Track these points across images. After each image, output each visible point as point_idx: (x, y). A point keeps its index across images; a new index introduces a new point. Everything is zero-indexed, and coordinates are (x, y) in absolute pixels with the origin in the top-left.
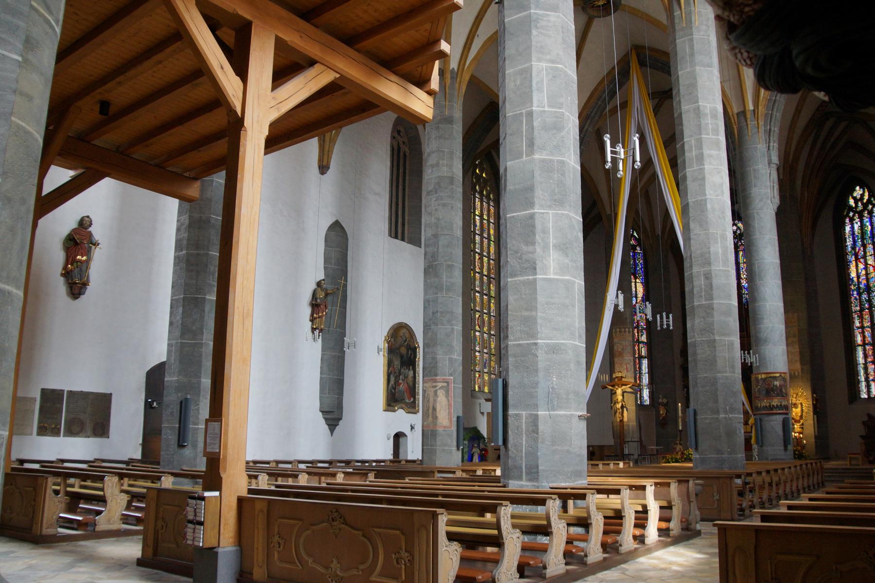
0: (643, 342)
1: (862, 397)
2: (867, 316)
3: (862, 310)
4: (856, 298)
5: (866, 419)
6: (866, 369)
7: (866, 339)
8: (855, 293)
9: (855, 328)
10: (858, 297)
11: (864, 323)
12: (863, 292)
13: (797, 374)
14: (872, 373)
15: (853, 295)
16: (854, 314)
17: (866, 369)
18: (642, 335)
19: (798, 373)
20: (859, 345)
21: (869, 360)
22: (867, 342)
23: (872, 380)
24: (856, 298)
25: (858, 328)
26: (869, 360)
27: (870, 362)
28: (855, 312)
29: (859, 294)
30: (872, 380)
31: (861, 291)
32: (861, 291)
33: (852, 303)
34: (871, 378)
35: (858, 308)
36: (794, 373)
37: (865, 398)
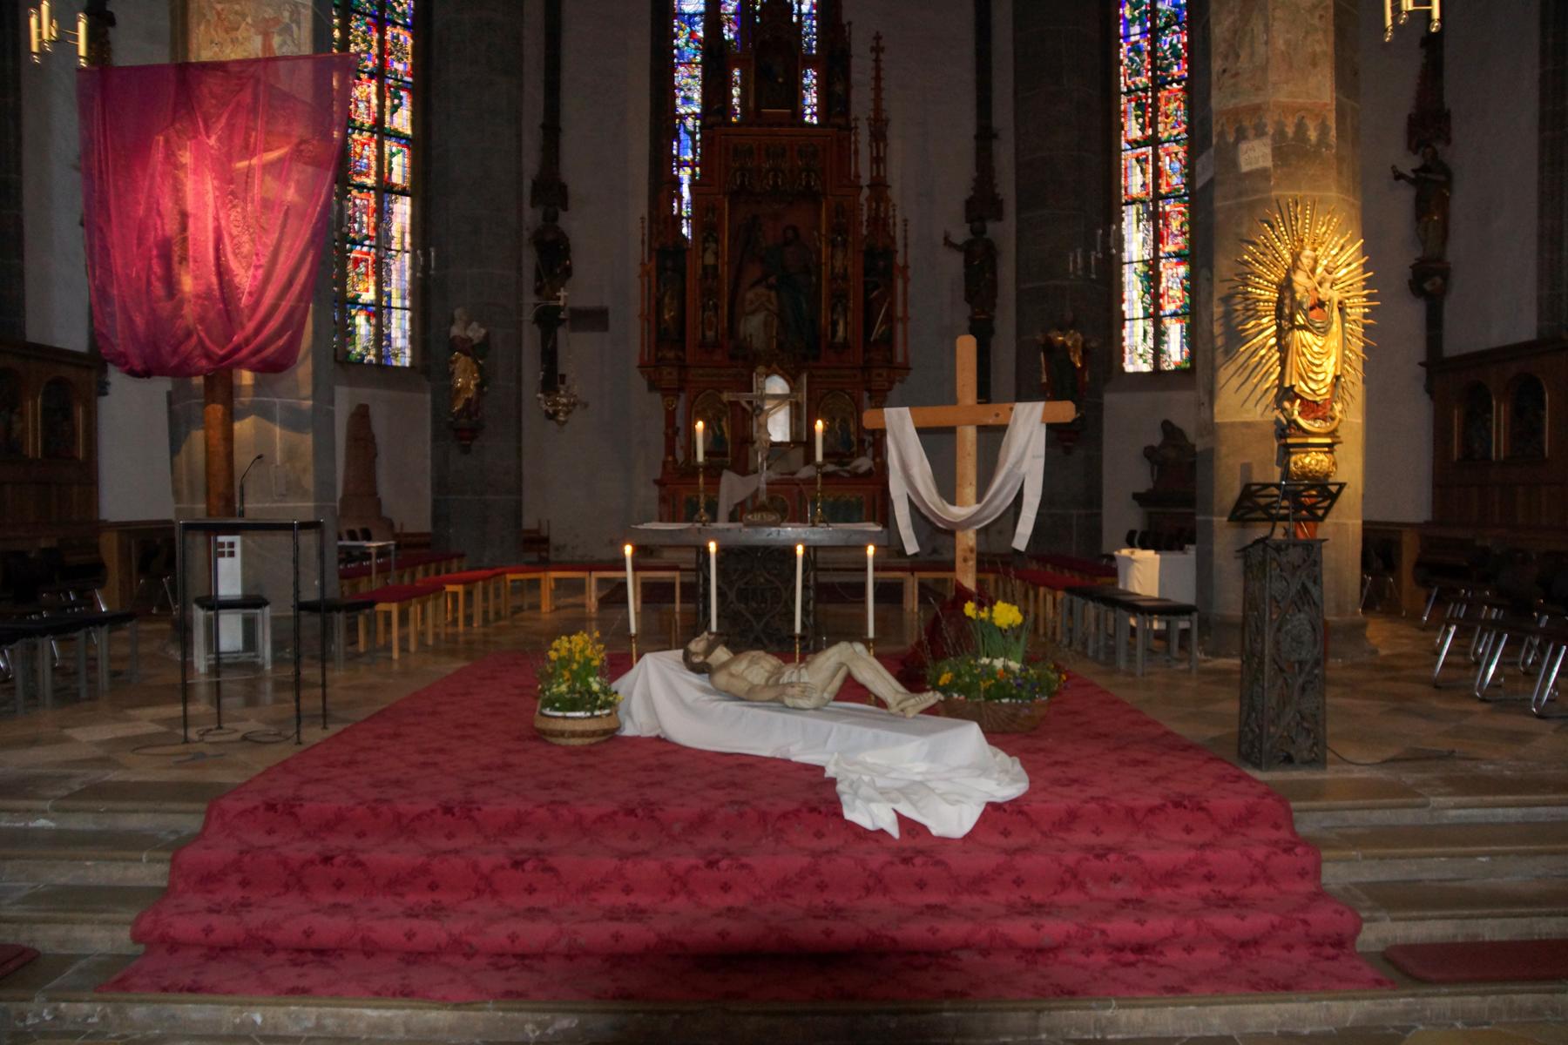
0: (397, 136)
1: (1129, 368)
2: (1173, 106)
3: (1158, 84)
4: (1135, 47)
5: (1156, 439)
6: (1152, 277)
7: (1163, 182)
8: (1136, 29)
9: (1124, 145)
10: (1145, 45)
11: (1161, 127)
12: (1168, 25)
13: (1313, 135)
14: (1176, 292)
15: (1127, 37)
16: (1124, 99)
17: (1152, 277)
18: (395, 109)
19: (1323, 130)
20: (1133, 202)
21: (1170, 247)
22: (1164, 190)
23: (1174, 315)
24: (1135, 47)
25: (1135, 144)
26: (1170, 247)
27: (1169, 256)
28: (1130, 92)
29: (1154, 34)
30: (1174, 315)
31: (1161, 23)
32: (1161, 23)
33: (1121, 63)
34: (1169, 308)
35: (1142, 81)
36: (1301, 127)
37: (1138, 375)
